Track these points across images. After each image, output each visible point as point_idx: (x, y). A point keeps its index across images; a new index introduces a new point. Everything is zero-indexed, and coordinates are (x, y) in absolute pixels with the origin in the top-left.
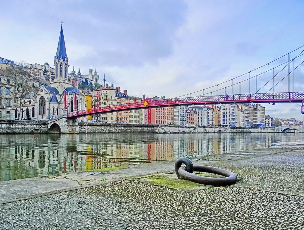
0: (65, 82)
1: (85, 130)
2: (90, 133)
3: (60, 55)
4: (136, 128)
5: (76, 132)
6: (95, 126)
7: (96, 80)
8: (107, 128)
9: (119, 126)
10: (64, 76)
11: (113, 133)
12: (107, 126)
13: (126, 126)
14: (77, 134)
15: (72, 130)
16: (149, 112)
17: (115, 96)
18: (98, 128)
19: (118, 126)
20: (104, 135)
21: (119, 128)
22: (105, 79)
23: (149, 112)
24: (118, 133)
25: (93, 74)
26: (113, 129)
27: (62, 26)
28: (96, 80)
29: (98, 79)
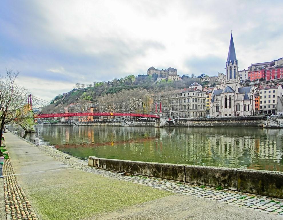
0: (229, 83)
1: (187, 124)
2: (190, 127)
3: (229, 60)
4: (231, 122)
5: (160, 126)
6: (194, 121)
8: (203, 122)
9: (214, 121)
11: (207, 126)
12: (203, 121)
13: (220, 120)
14: (160, 127)
15: (158, 125)
18: (196, 122)
21: (213, 122)
24: (211, 126)
26: (208, 123)
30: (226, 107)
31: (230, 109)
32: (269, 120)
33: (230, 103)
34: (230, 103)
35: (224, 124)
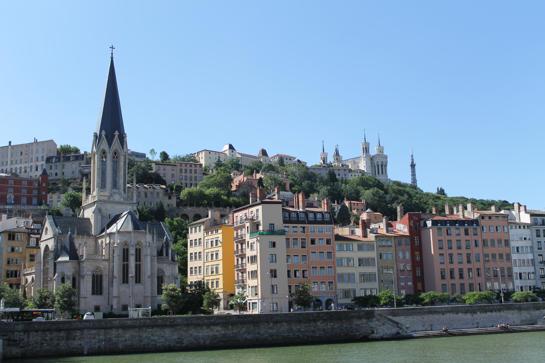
7: (380, 167)
10: (109, 185)
16: (418, 258)
17: (285, 222)
19: (199, 325)
20: (431, 316)
22: (413, 162)
23: (418, 258)
25: (373, 151)
27: (112, 58)
28: (380, 167)
29: (386, 166)
30: (125, 279)
31: (138, 287)
32: (378, 320)
33: (138, 268)
34: (138, 268)
35: (249, 337)
